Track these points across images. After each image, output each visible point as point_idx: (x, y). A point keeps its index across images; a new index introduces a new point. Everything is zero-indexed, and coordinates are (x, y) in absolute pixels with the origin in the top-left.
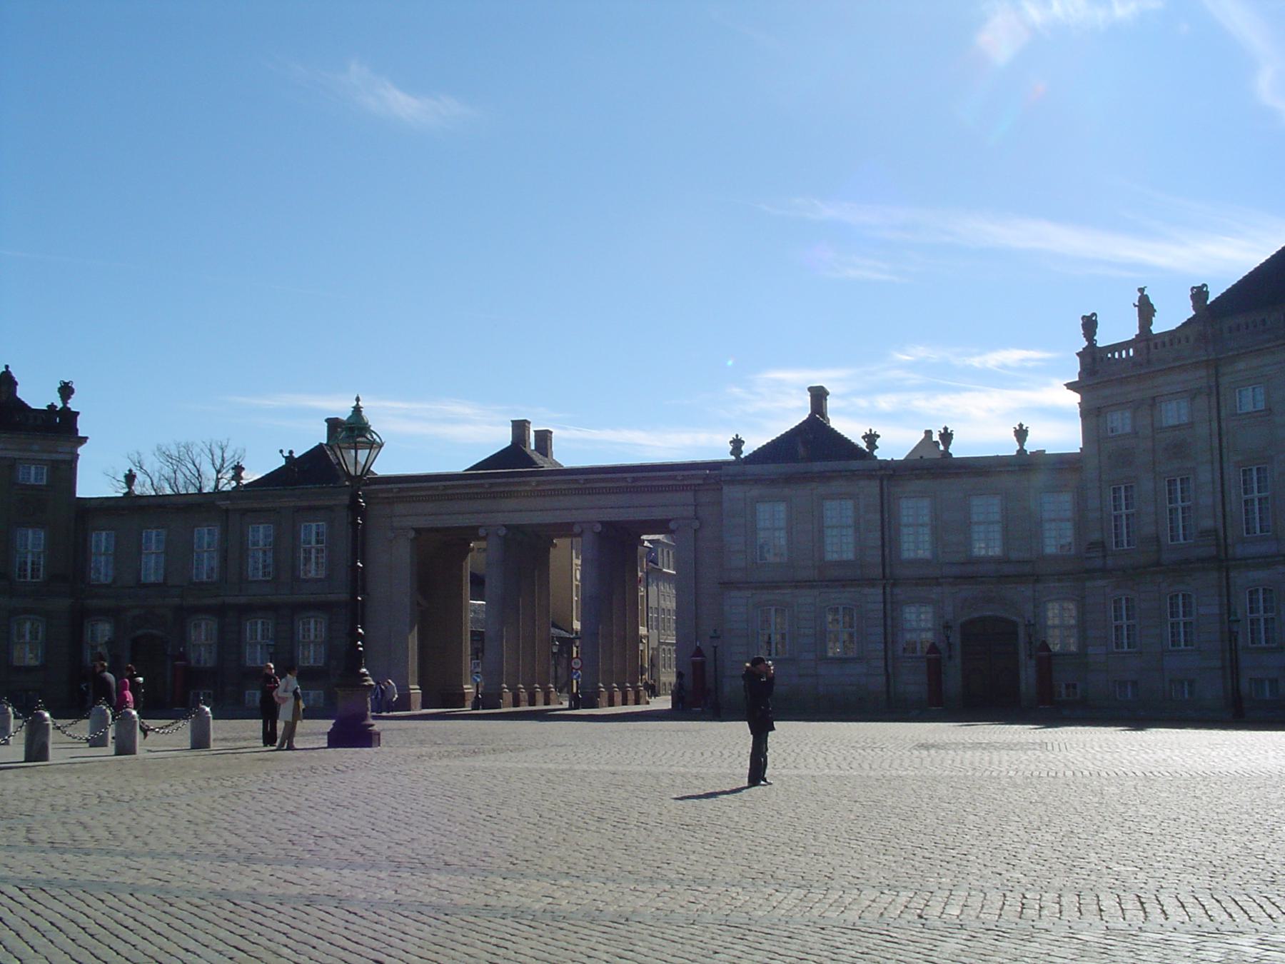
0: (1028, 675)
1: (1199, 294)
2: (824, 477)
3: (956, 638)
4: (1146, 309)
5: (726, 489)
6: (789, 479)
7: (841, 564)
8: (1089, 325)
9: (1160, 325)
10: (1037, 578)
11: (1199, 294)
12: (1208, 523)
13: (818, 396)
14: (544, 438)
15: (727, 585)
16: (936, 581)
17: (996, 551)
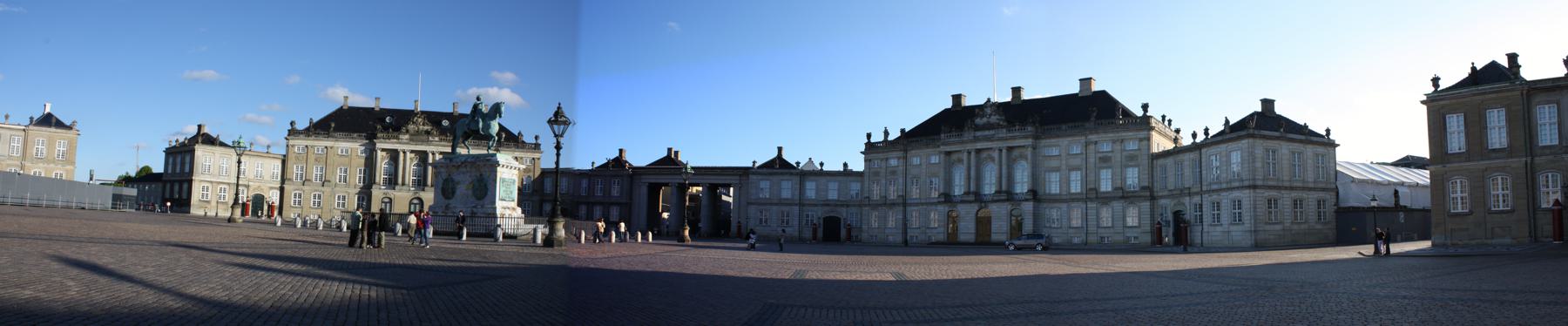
0: (843, 233)
1: (903, 131)
2: (782, 174)
3: (822, 222)
4: (886, 133)
5: (750, 176)
6: (771, 174)
7: (787, 199)
8: (869, 136)
9: (891, 138)
10: (848, 206)
11: (903, 131)
12: (900, 193)
13: (780, 149)
14: (676, 153)
15: (749, 204)
16: (816, 205)
17: (836, 197)
